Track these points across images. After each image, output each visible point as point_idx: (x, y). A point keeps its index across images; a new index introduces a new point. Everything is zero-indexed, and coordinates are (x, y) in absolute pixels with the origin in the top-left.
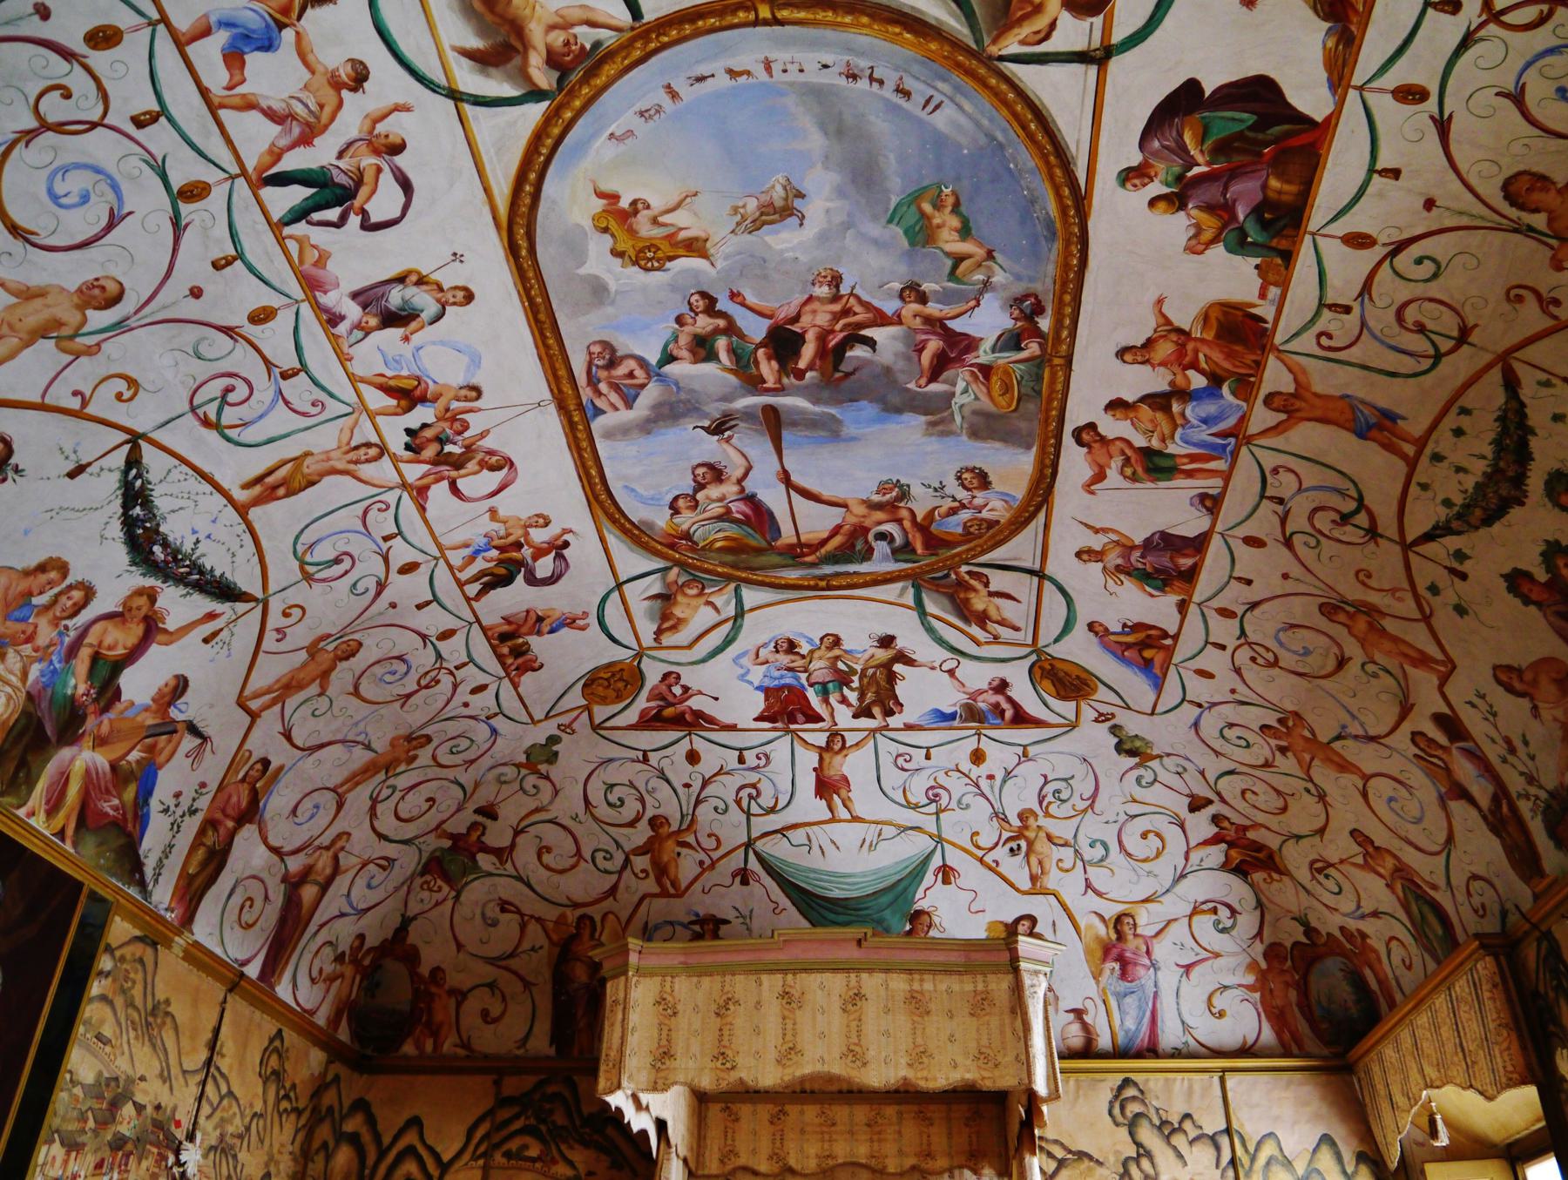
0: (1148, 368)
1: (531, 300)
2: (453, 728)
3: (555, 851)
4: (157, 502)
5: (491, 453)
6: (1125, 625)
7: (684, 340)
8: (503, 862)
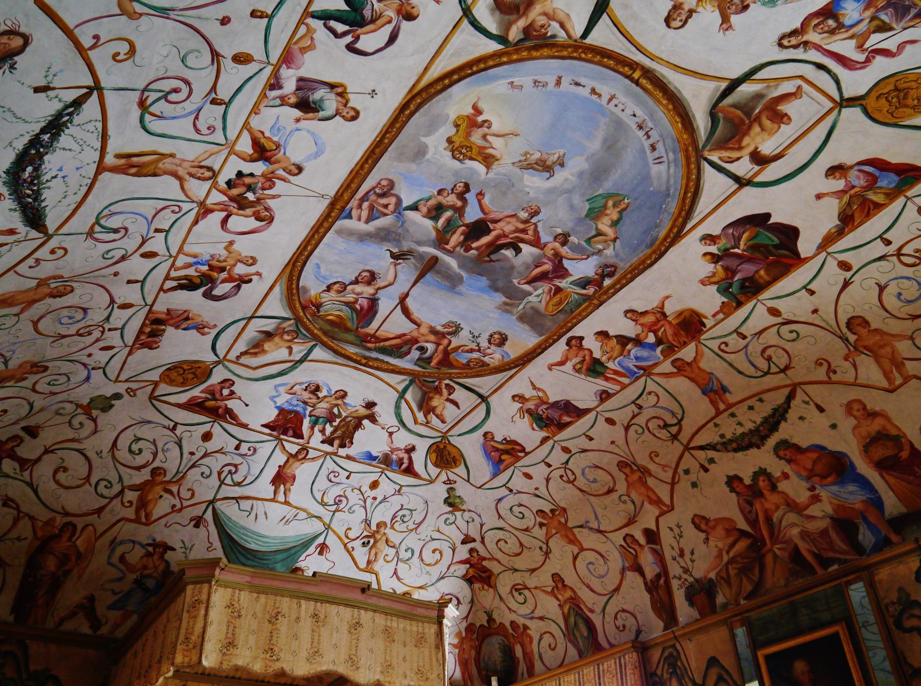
0: (634, 323)
1: (383, 138)
2: (66, 367)
3: (70, 472)
5: (267, 209)
6: (505, 439)
7: (432, 202)
8: (22, 469)
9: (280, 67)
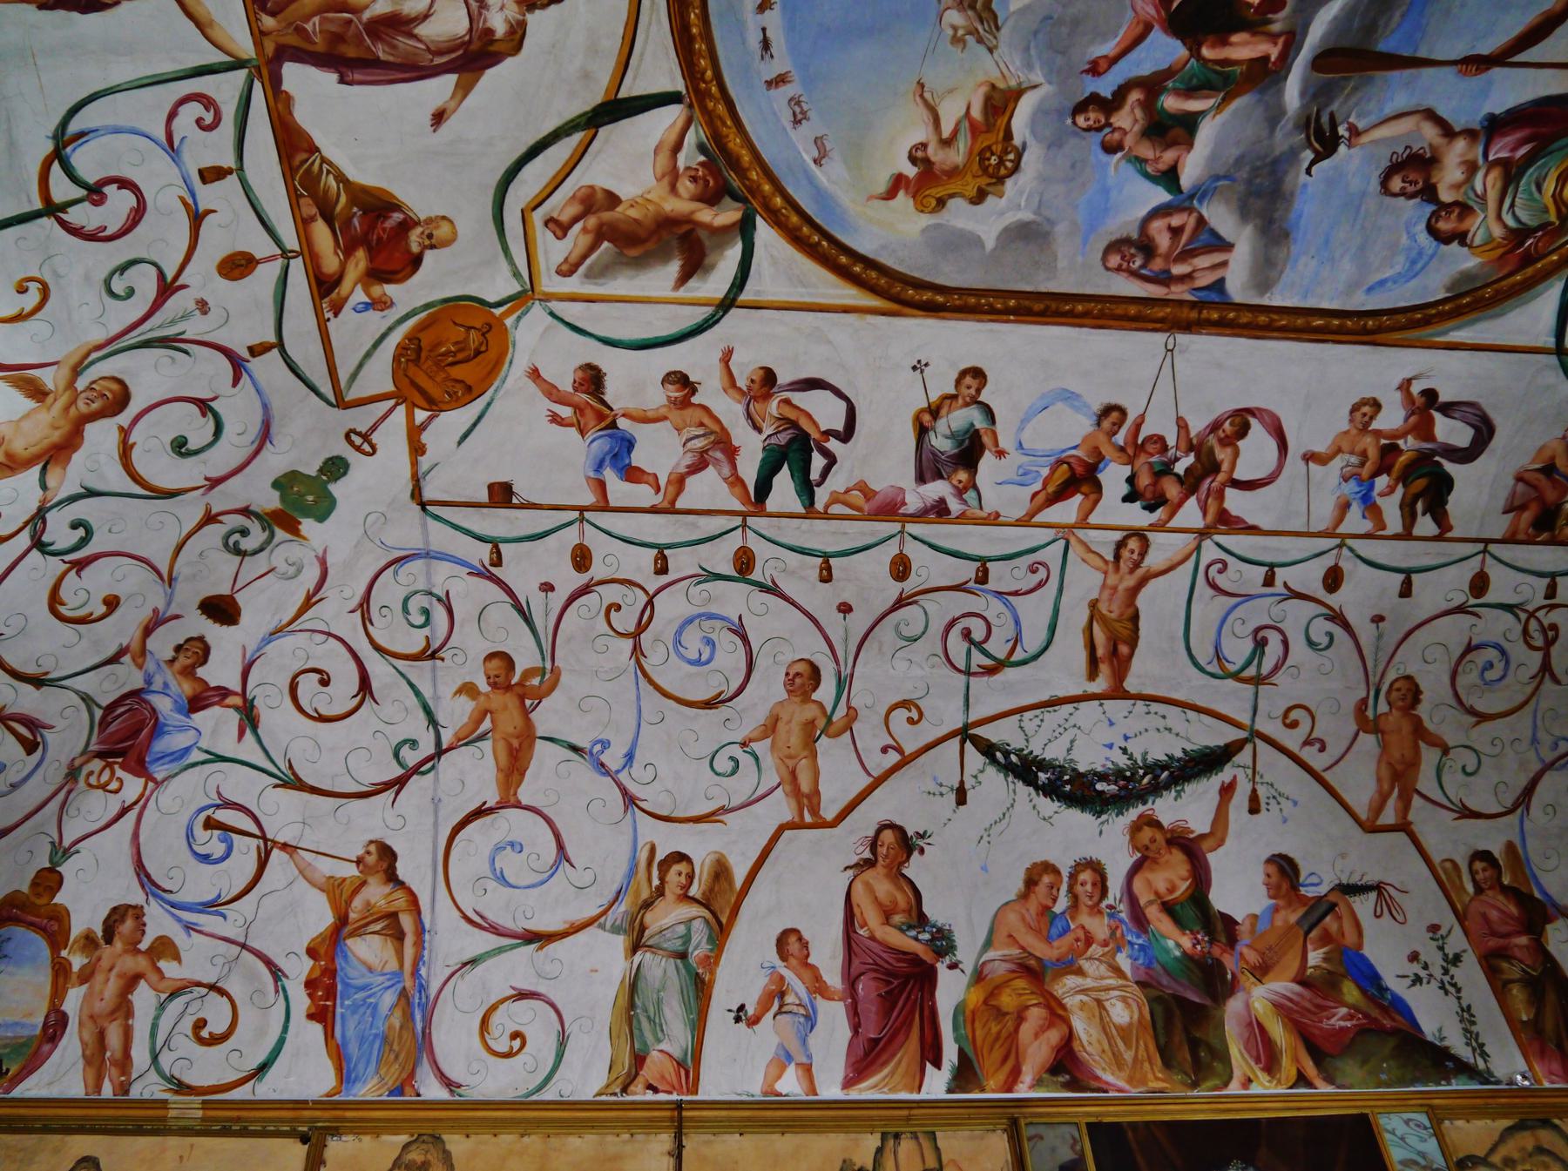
4: (1048, 755)
5: (1215, 426)
7: (1146, 151)
9: (905, 515)
